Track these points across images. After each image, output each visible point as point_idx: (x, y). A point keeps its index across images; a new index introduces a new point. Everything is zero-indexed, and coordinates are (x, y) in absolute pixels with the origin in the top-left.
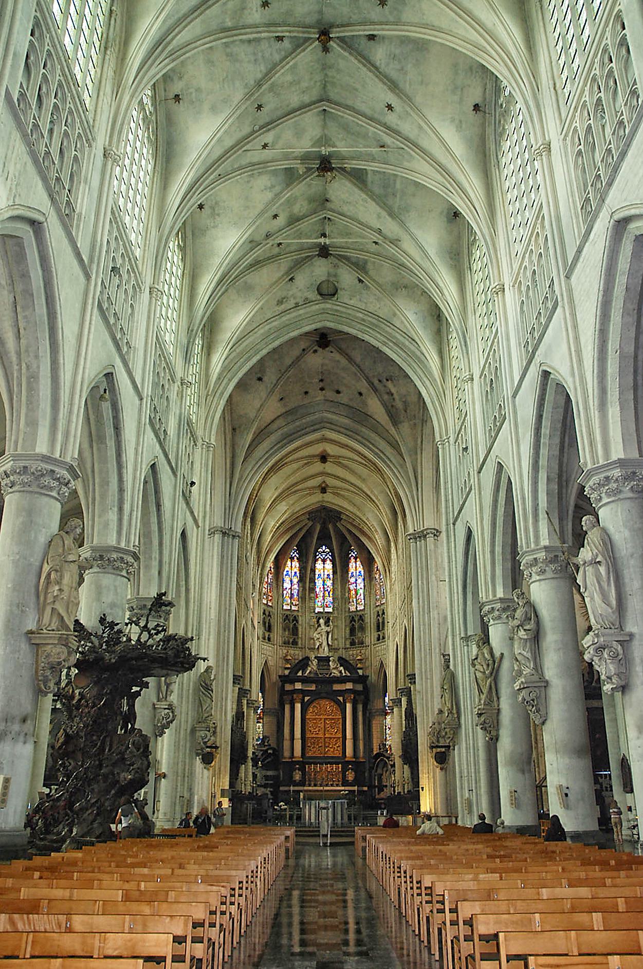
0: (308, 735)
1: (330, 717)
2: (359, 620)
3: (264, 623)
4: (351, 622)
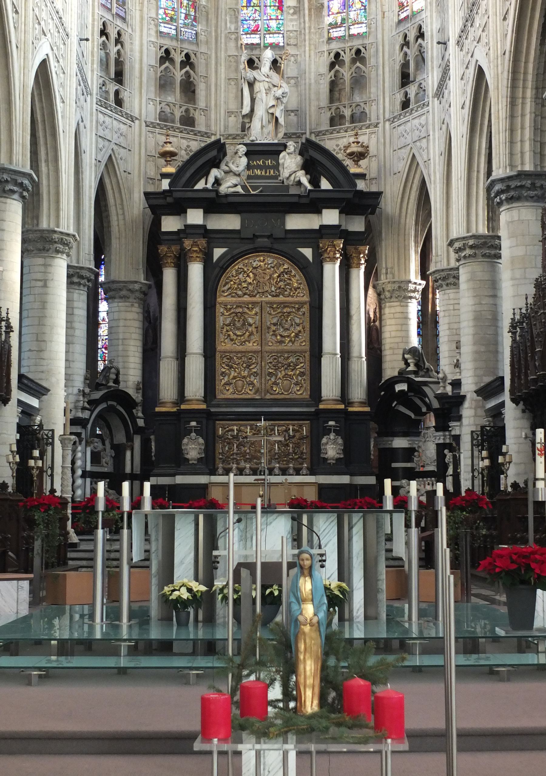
0: (220, 347)
1: (281, 298)
2: (353, 61)
3: (105, 64)
4: (332, 65)
